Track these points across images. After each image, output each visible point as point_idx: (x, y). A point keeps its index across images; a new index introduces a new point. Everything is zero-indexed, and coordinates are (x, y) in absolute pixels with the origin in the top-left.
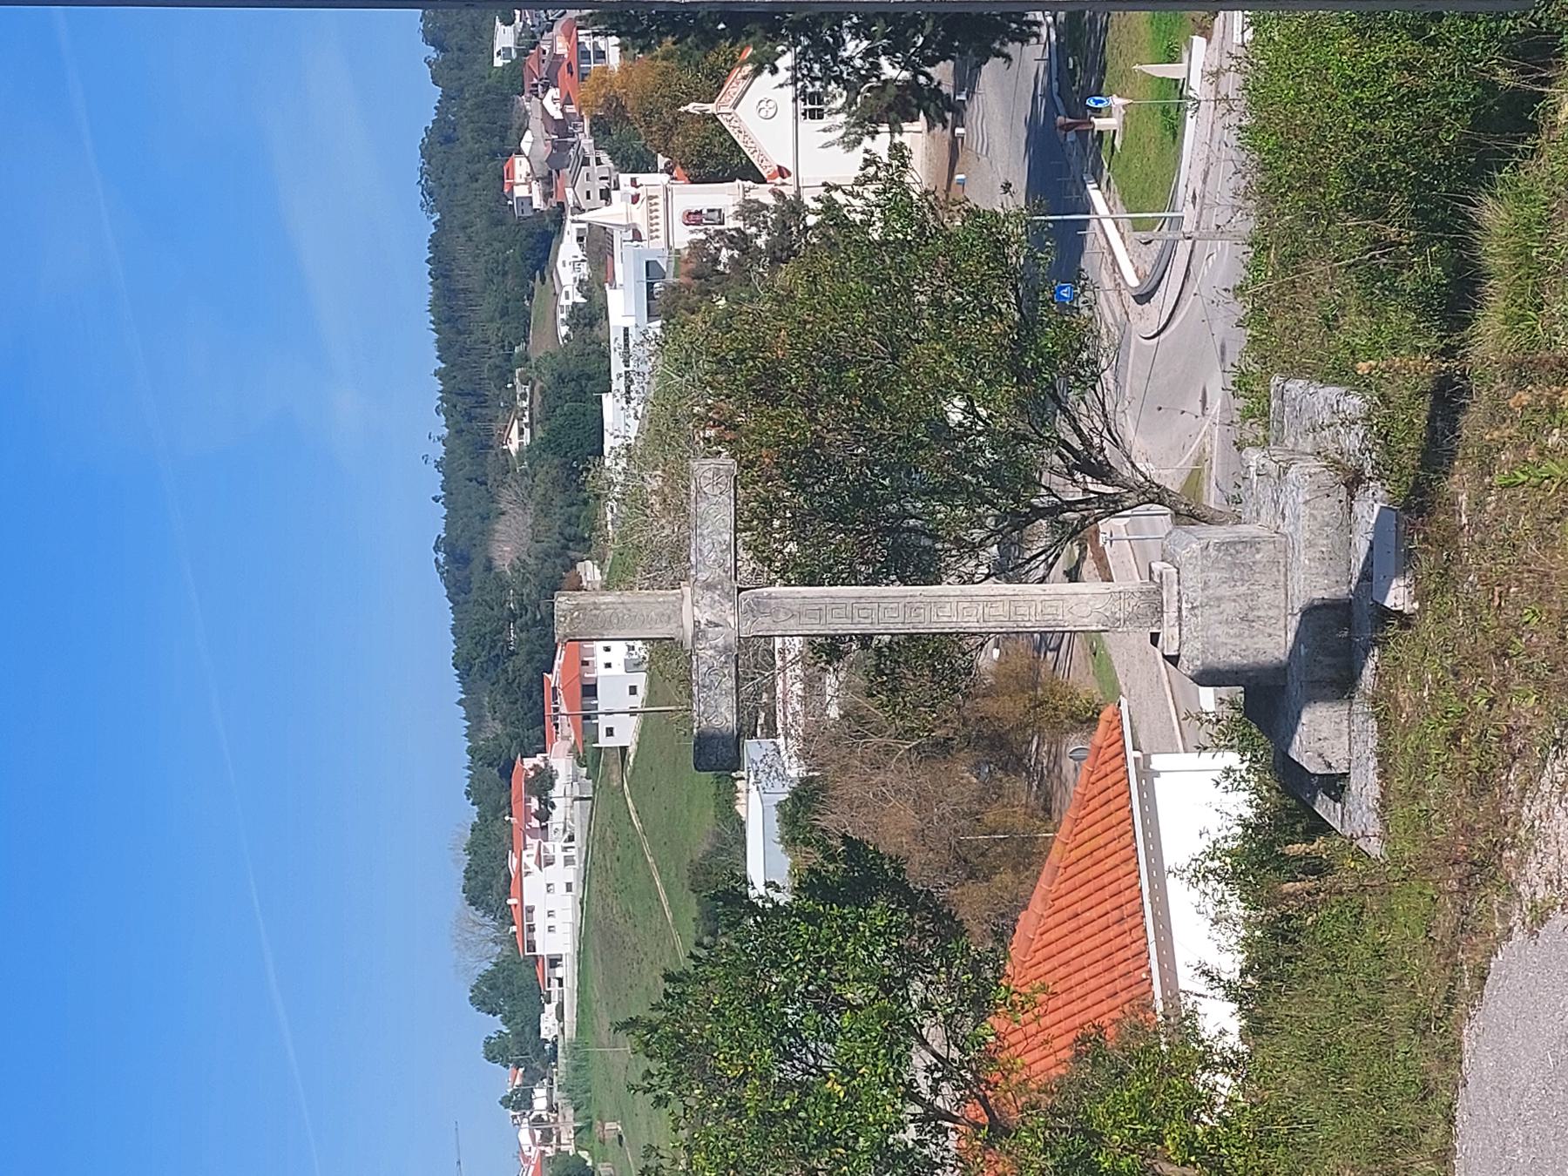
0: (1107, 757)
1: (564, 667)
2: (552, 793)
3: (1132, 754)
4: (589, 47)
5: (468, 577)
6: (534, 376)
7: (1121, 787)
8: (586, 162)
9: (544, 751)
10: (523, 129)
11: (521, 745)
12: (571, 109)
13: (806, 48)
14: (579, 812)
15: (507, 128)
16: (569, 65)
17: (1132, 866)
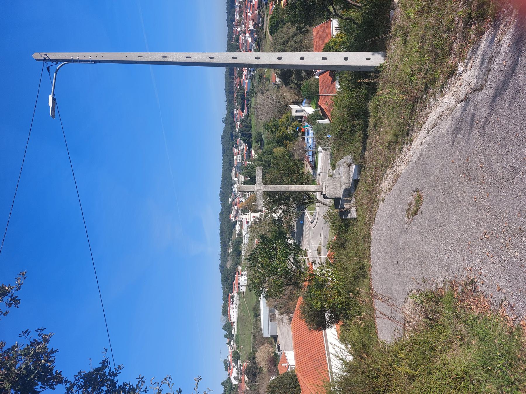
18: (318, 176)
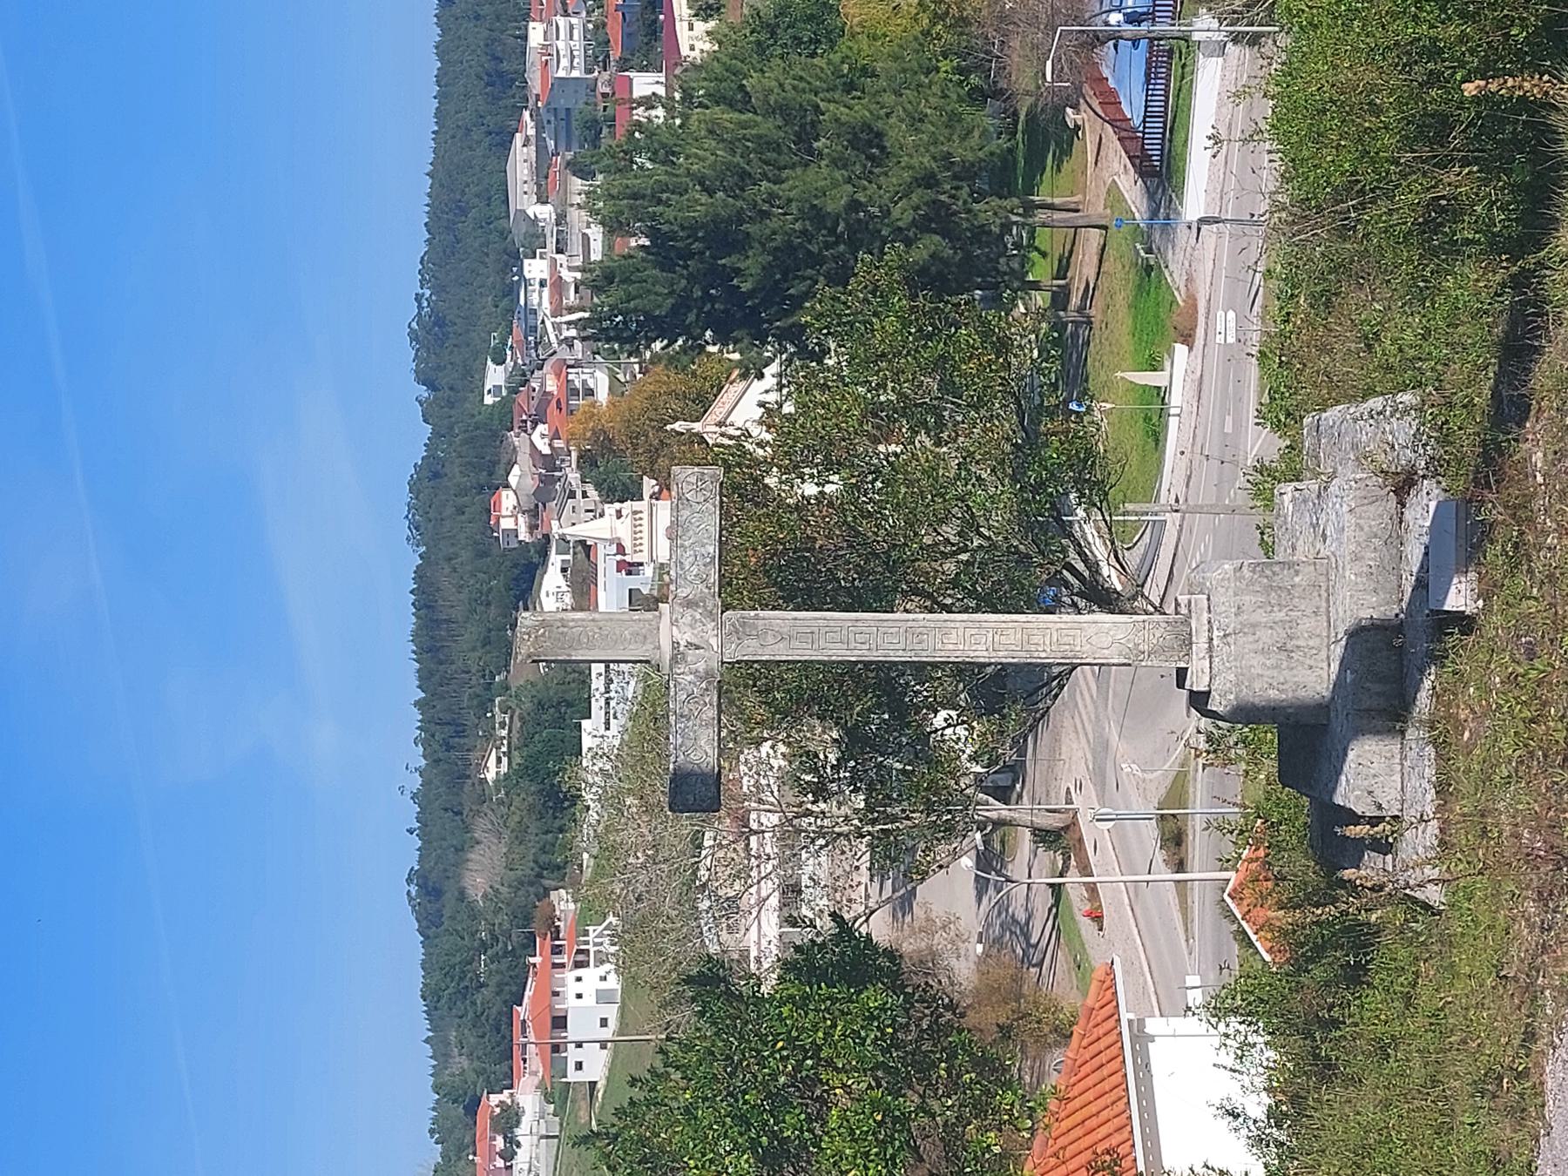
0: (1099, 1019)
1: (533, 998)
2: (518, 1131)
3: (1125, 1016)
4: (578, 384)
5: (439, 911)
6: (513, 703)
7: (1114, 1050)
8: (572, 495)
9: (511, 1087)
10: (511, 465)
11: (488, 1081)
12: (558, 444)
13: (792, 354)
14: (546, 1150)
15: (495, 463)
16: (558, 401)
17: (1125, 1135)
18: (1183, 237)
